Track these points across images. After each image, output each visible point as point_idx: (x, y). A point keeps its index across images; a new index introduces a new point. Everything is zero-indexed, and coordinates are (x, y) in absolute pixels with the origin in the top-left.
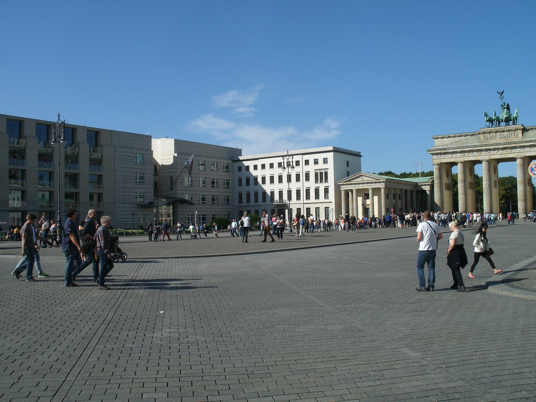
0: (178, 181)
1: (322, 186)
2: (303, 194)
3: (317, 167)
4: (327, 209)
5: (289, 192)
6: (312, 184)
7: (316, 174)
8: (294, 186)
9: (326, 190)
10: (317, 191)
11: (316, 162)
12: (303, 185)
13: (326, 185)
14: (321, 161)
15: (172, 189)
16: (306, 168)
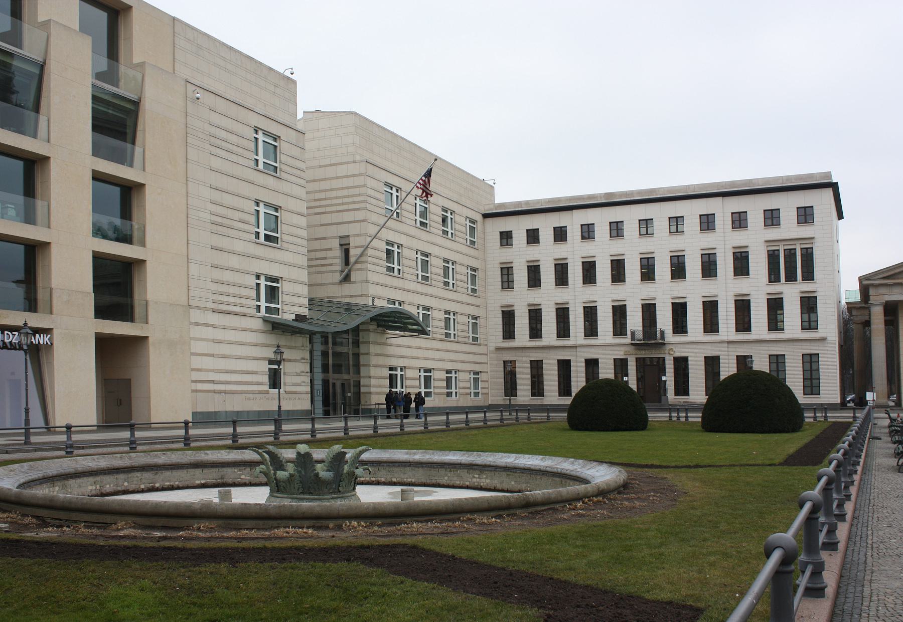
0: (370, 252)
1: (791, 294)
2: (727, 316)
3: (773, 234)
4: (811, 363)
5: (679, 311)
6: (757, 286)
7: (773, 257)
8: (694, 290)
9: (809, 305)
10: (775, 306)
11: (772, 218)
12: (726, 288)
13: (807, 286)
14: (788, 216)
15: (346, 279)
16: (740, 238)
